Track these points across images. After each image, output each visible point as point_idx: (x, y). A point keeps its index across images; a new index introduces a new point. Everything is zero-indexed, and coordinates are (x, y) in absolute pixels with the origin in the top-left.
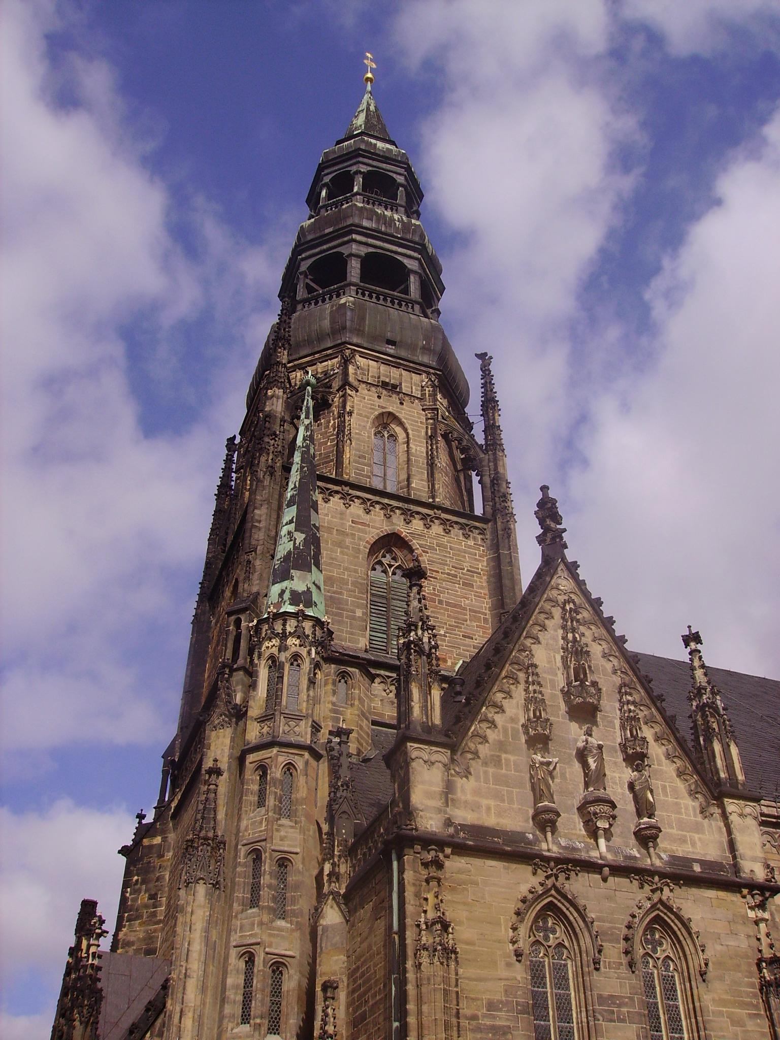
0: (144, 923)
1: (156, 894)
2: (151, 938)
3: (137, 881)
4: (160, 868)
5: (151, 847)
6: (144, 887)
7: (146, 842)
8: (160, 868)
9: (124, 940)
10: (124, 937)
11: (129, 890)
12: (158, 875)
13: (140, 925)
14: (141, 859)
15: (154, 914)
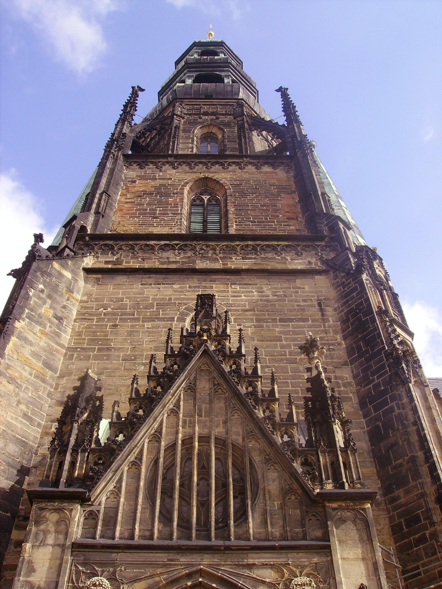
0: (46, 334)
1: (62, 319)
2: (52, 354)
3: (42, 291)
4: (68, 300)
5: (61, 275)
6: (49, 302)
7: (56, 265)
8: (68, 300)
9: (21, 332)
10: (22, 330)
11: (32, 290)
12: (65, 303)
13: (43, 333)
14: (50, 275)
15: (58, 335)
